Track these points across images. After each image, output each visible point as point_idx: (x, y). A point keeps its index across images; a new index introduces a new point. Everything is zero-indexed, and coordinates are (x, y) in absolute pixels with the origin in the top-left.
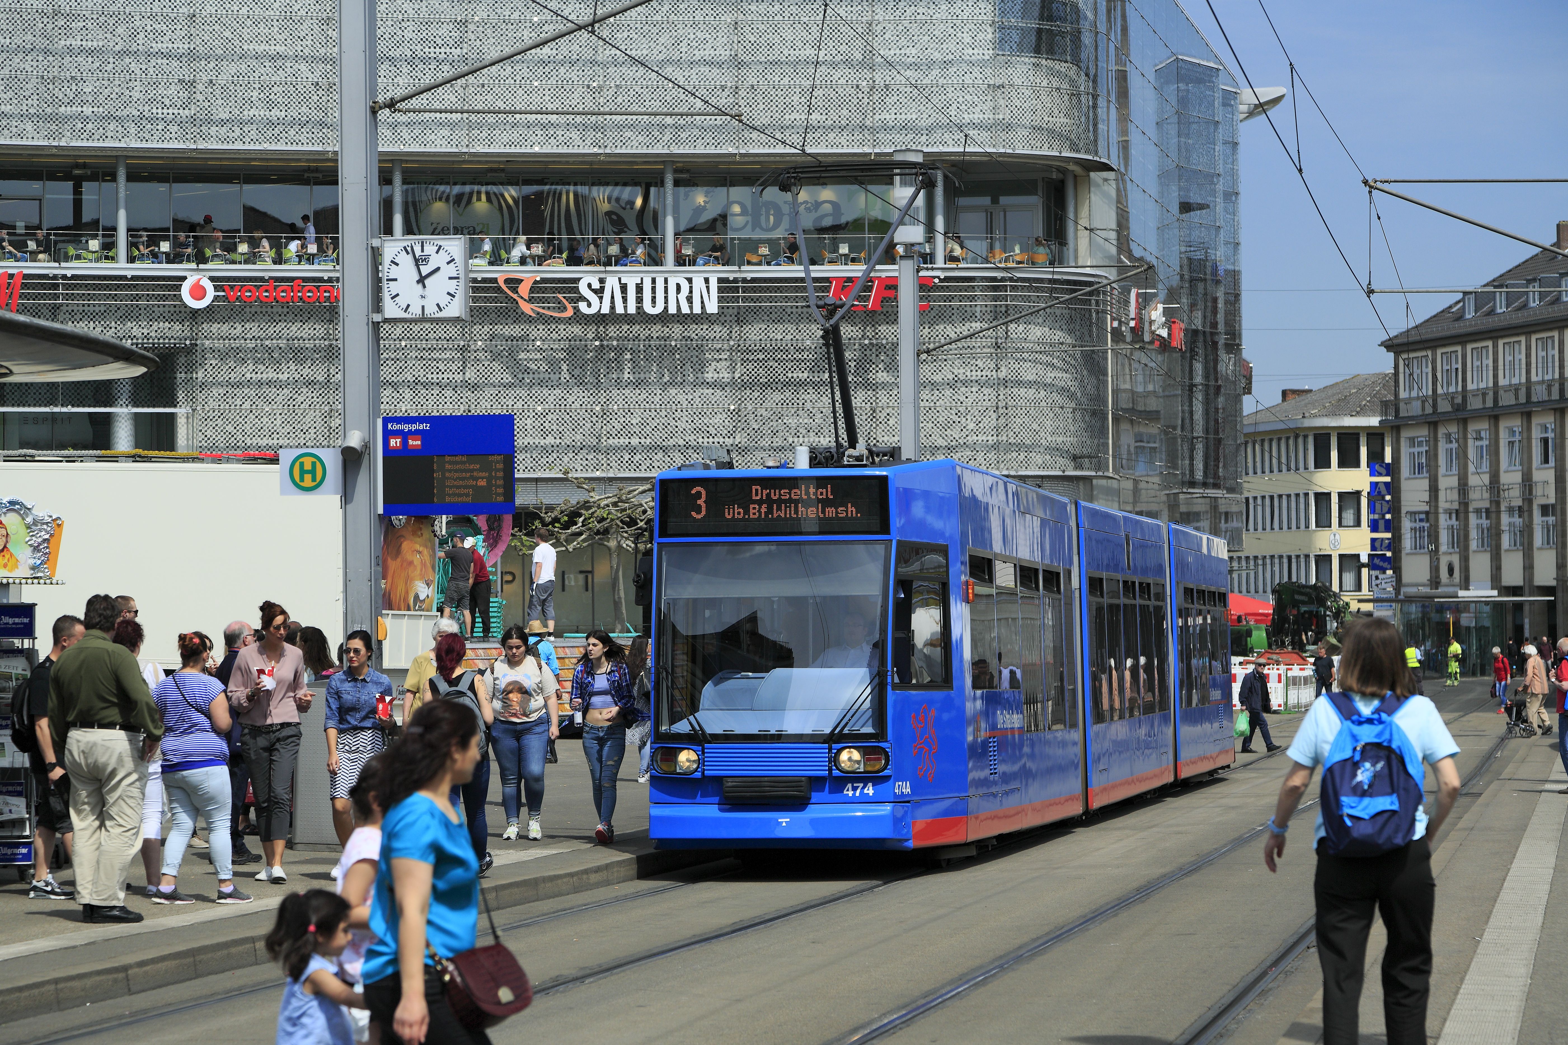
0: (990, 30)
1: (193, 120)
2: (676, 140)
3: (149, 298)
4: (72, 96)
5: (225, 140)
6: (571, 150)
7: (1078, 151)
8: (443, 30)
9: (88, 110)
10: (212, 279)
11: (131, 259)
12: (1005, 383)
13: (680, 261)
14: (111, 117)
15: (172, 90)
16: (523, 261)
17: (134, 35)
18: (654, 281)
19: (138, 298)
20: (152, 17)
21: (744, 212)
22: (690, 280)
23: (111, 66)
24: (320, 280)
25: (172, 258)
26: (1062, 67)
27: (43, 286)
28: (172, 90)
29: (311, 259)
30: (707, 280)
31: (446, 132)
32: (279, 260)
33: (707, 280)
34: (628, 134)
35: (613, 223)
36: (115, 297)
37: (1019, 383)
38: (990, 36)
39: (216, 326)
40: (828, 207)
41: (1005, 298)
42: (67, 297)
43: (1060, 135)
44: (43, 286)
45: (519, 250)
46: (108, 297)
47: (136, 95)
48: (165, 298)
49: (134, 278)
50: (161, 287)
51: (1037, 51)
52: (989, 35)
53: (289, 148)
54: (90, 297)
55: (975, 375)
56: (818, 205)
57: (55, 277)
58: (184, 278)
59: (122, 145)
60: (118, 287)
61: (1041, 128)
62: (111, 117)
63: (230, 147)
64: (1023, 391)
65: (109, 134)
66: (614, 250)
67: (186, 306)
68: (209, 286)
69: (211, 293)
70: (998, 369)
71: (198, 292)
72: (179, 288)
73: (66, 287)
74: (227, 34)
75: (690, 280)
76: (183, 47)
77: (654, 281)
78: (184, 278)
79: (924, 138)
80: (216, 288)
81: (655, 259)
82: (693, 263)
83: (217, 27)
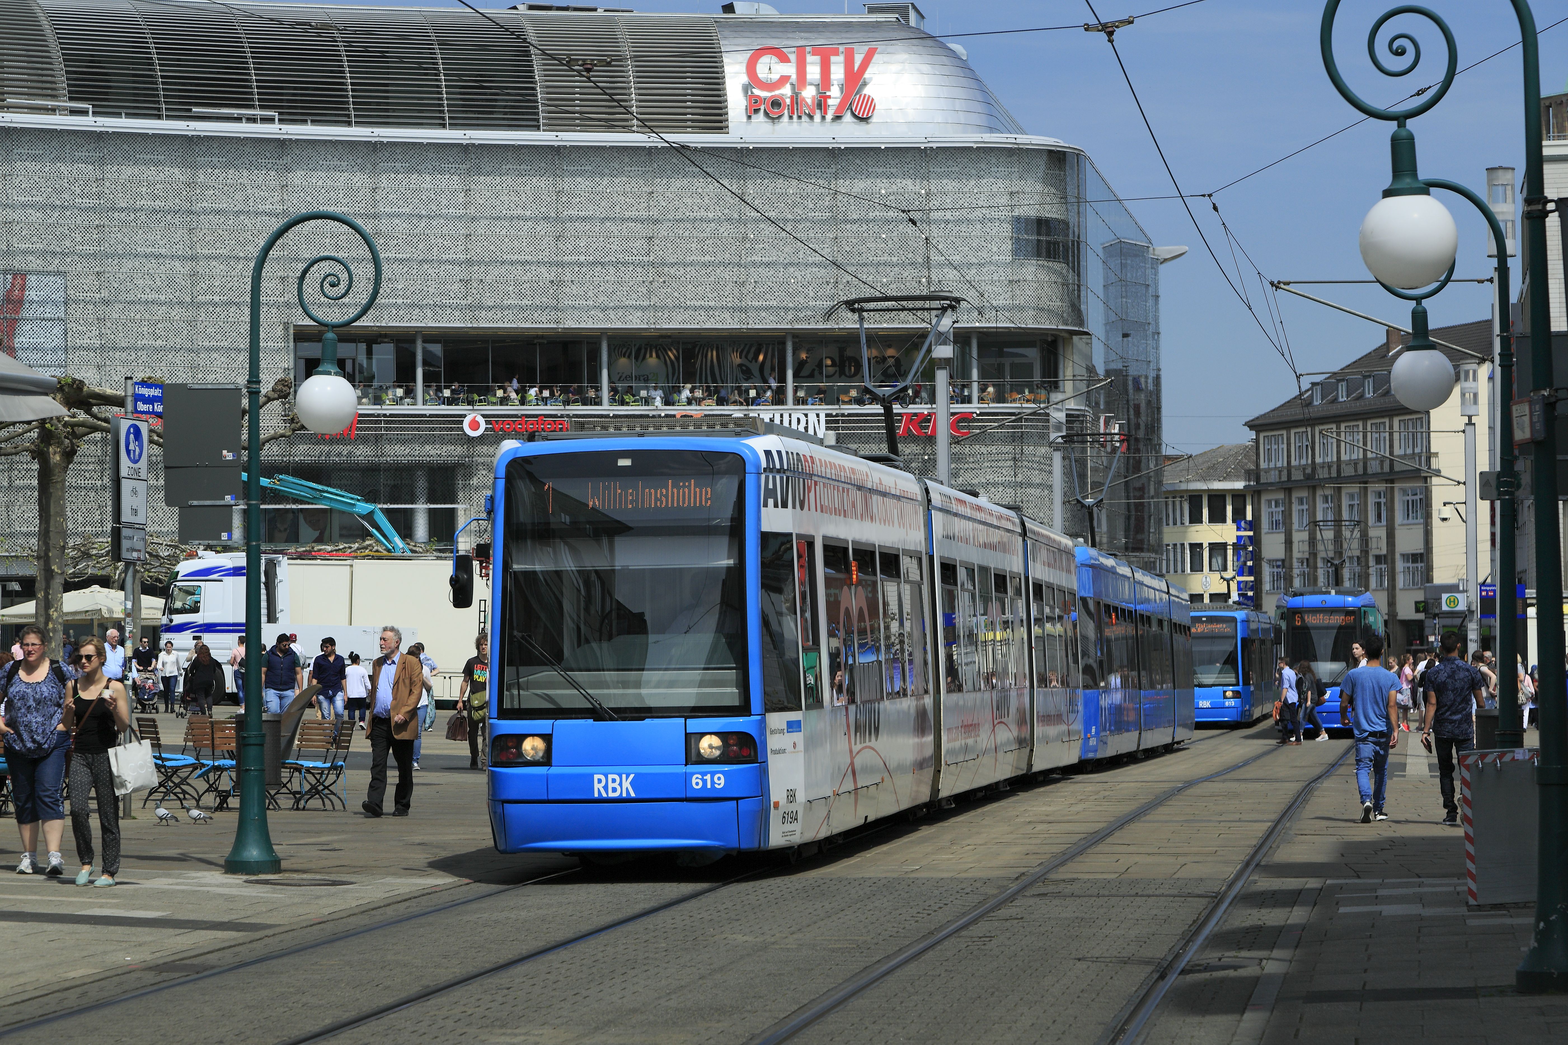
0: (1010, 243)
1: (470, 307)
2: (797, 320)
3: (441, 429)
4: (388, 291)
5: (493, 321)
6: (724, 327)
7: (1067, 324)
8: (638, 244)
9: (400, 301)
10: (484, 416)
11: (425, 402)
12: (1021, 485)
13: (798, 401)
14: (413, 306)
15: (456, 287)
16: (689, 402)
17: (430, 250)
18: (782, 416)
19: (434, 429)
20: (442, 236)
21: (834, 364)
22: (806, 415)
23: (415, 271)
24: (555, 416)
25: (450, 402)
26: (1057, 266)
27: (371, 422)
28: (456, 287)
29: (545, 401)
30: (818, 415)
31: (639, 314)
32: (523, 402)
33: (818, 415)
34: (763, 314)
35: (743, 372)
36: (418, 429)
37: (1030, 485)
38: (1010, 247)
39: (485, 448)
40: (891, 361)
41: (1021, 427)
42: (387, 429)
43: (1057, 314)
44: (371, 422)
45: (686, 394)
46: (414, 429)
47: (431, 290)
48: (452, 429)
49: (431, 416)
50: (449, 422)
51: (1039, 255)
52: (1008, 246)
53: (534, 326)
54: (402, 429)
55: (1001, 479)
56: (884, 359)
57: (379, 415)
58: (465, 416)
59: (423, 325)
60: (420, 422)
61: (1042, 309)
62: (413, 306)
63: (495, 325)
64: (1032, 491)
65: (414, 317)
66: (753, 393)
67: (465, 434)
68: (482, 421)
69: (483, 426)
70: (1015, 475)
71: (475, 425)
72: (461, 422)
73: (387, 422)
74: (492, 247)
75: (806, 415)
76: (463, 257)
77: (782, 416)
78: (465, 416)
79: (965, 317)
80: (487, 422)
81: (779, 399)
82: (804, 402)
83: (485, 243)
